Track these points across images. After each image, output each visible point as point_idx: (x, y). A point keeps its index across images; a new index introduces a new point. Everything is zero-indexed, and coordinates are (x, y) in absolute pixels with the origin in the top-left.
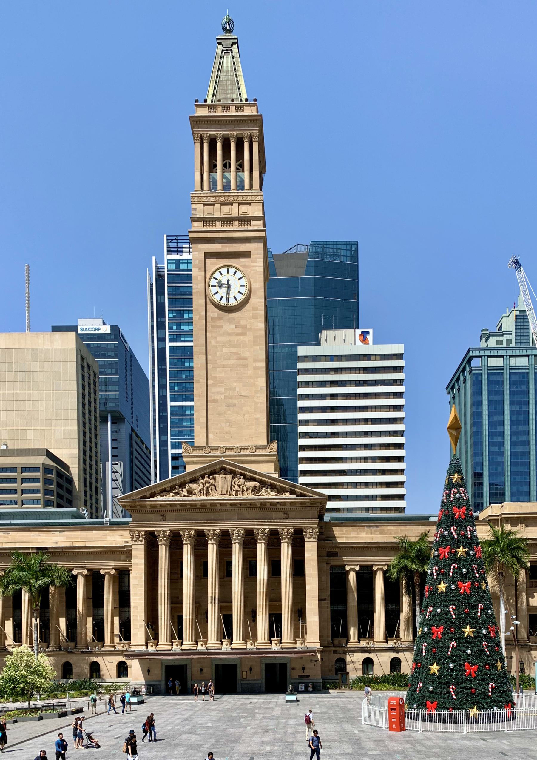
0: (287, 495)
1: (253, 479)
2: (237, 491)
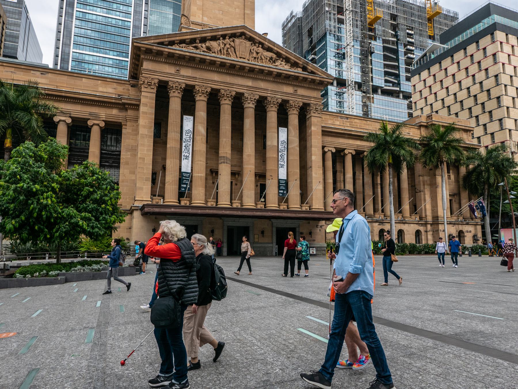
0: (300, 70)
1: (269, 50)
2: (255, 58)
